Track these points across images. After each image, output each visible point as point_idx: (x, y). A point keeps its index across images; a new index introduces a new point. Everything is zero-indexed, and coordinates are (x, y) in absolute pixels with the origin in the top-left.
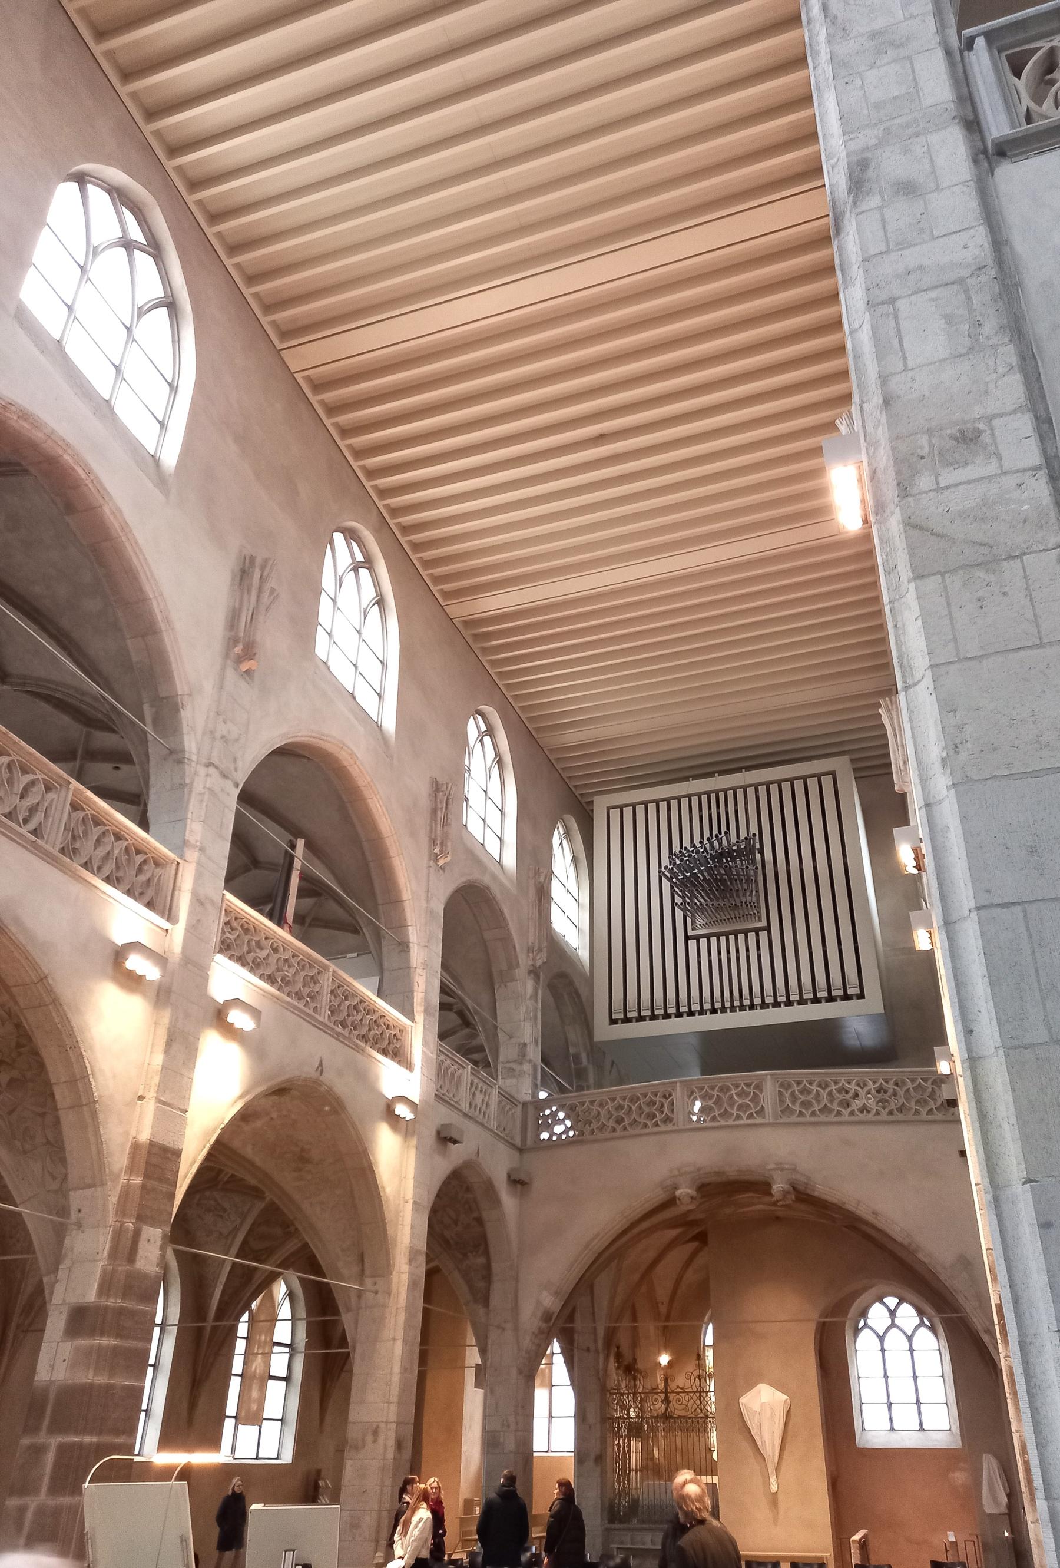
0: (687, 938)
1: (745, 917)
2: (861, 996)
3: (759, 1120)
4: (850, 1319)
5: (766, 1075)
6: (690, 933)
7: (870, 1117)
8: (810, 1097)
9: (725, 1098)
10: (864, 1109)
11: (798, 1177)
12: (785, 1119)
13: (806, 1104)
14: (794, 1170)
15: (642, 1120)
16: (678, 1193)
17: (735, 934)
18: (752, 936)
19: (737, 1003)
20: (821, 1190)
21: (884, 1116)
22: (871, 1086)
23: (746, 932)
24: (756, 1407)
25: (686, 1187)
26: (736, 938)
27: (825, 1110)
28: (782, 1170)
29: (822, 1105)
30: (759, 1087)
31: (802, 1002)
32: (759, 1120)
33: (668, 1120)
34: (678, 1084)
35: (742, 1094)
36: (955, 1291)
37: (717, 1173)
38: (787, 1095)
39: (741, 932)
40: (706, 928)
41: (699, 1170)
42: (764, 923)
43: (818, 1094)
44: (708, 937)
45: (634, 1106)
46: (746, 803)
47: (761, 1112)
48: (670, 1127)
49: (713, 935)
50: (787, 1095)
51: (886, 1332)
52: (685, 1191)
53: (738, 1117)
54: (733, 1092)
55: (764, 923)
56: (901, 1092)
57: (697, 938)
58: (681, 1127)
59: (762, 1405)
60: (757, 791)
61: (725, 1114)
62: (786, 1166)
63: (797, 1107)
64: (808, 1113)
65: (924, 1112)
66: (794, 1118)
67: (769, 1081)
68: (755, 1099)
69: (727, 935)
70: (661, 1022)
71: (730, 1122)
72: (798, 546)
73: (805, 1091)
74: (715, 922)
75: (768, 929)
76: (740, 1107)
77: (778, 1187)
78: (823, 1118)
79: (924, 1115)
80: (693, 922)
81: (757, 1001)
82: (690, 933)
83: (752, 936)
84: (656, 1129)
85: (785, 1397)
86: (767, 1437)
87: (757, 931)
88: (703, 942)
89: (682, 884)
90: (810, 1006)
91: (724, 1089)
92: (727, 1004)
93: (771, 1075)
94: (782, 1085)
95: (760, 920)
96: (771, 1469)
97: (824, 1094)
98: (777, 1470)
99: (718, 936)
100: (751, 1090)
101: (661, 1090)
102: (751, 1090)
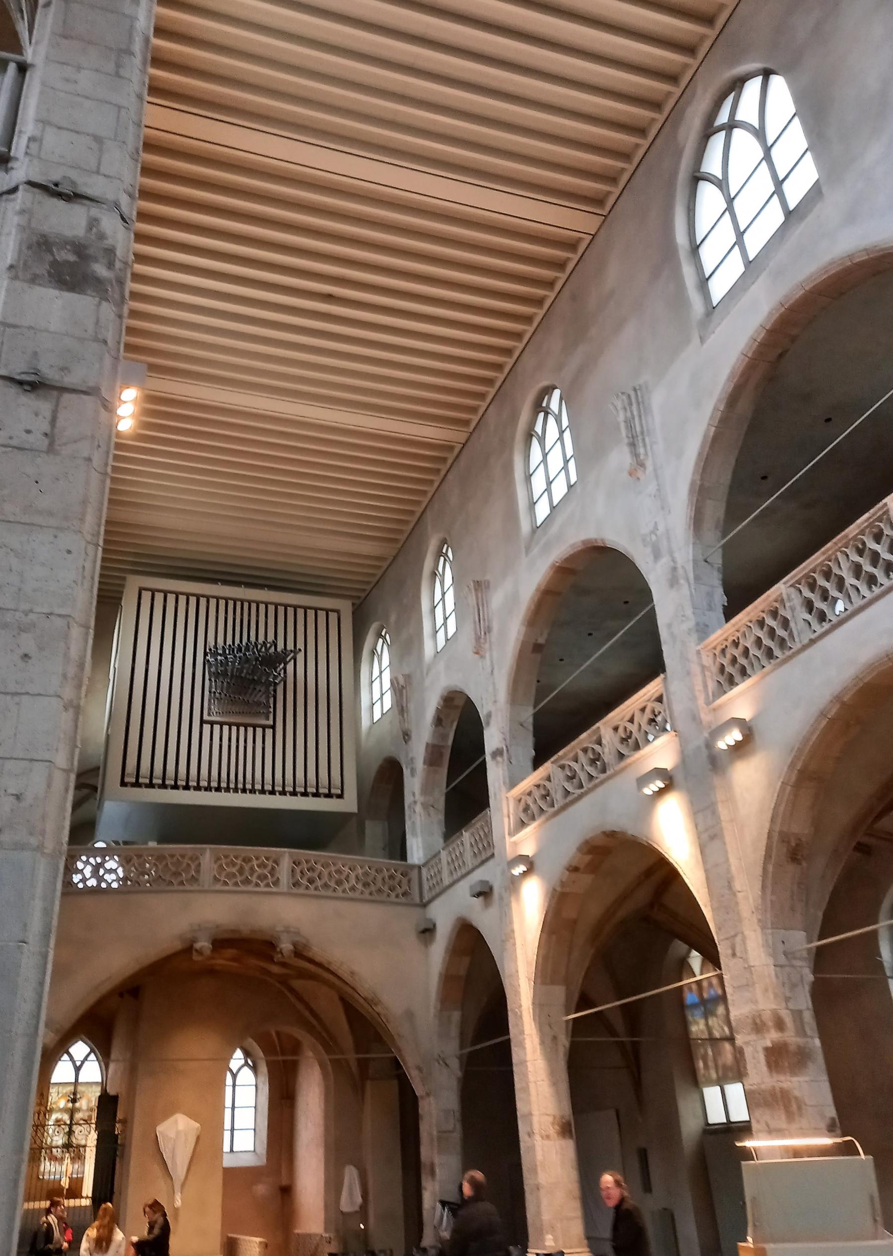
0: (202, 722)
1: (257, 714)
2: (340, 796)
3: (274, 889)
4: (113, 1061)
5: (285, 852)
6: (206, 717)
7: (357, 895)
8: (315, 875)
9: (247, 868)
10: (353, 889)
11: (297, 939)
12: (295, 890)
13: (311, 881)
14: (298, 933)
15: (167, 877)
16: (198, 945)
17: (246, 726)
18: (259, 731)
19: (240, 786)
20: (318, 952)
21: (367, 896)
22: (360, 871)
23: (246, 726)
24: (172, 1135)
25: (205, 941)
26: (246, 730)
27: (326, 886)
28: (288, 932)
29: (323, 881)
30: (276, 862)
31: (294, 793)
32: (274, 889)
33: (194, 879)
34: (208, 850)
35: (262, 866)
36: (399, 1035)
37: (233, 931)
38: (298, 870)
39: (251, 725)
40: (220, 716)
41: (217, 927)
42: (271, 722)
43: (242, 867)
44: (222, 724)
45: (160, 864)
46: (258, 616)
47: (276, 883)
48: (195, 887)
49: (226, 723)
50: (298, 870)
51: (239, 1069)
52: (203, 944)
53: (257, 885)
54: (255, 863)
55: (271, 722)
56: (379, 877)
57: (212, 723)
58: (206, 887)
59: (178, 1133)
60: (208, 602)
61: (247, 881)
62: (292, 930)
63: (304, 882)
64: (312, 887)
65: (393, 895)
66: (301, 891)
67: (286, 856)
68: (272, 871)
69: (238, 726)
70: (181, 792)
71: (250, 888)
72: (417, 438)
73: (311, 869)
74: (228, 713)
75: (273, 727)
76: (259, 877)
77: (286, 946)
78: (323, 892)
79: (393, 898)
80: (210, 709)
81: (258, 787)
82: (206, 717)
83: (250, 730)
84: (181, 888)
85: (197, 1125)
86: (178, 1162)
87: (264, 727)
88: (217, 728)
89: (216, 675)
90: (299, 798)
91: (247, 860)
92: (232, 786)
93: (289, 853)
94: (294, 863)
95: (268, 719)
96: (177, 1187)
97: (325, 872)
98: (183, 1185)
99: (222, 724)
100: (270, 863)
101: (190, 854)
102: (270, 863)
